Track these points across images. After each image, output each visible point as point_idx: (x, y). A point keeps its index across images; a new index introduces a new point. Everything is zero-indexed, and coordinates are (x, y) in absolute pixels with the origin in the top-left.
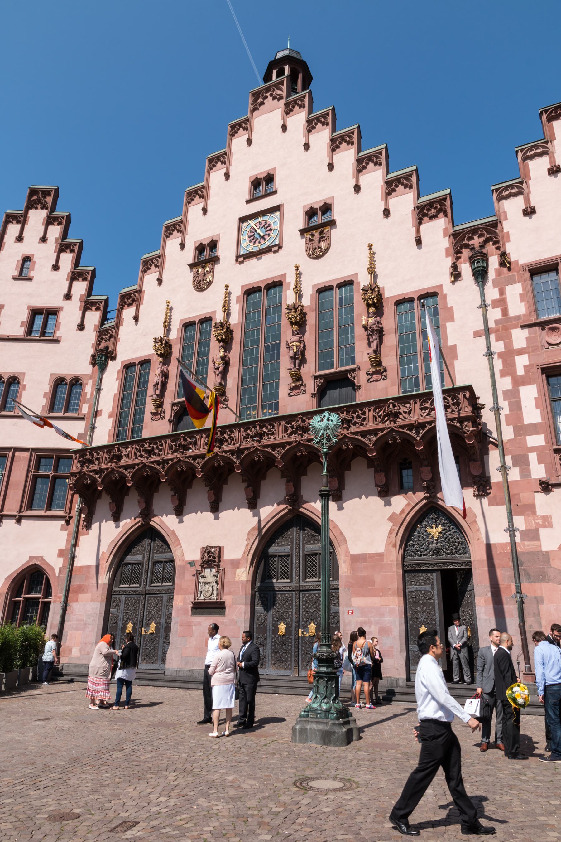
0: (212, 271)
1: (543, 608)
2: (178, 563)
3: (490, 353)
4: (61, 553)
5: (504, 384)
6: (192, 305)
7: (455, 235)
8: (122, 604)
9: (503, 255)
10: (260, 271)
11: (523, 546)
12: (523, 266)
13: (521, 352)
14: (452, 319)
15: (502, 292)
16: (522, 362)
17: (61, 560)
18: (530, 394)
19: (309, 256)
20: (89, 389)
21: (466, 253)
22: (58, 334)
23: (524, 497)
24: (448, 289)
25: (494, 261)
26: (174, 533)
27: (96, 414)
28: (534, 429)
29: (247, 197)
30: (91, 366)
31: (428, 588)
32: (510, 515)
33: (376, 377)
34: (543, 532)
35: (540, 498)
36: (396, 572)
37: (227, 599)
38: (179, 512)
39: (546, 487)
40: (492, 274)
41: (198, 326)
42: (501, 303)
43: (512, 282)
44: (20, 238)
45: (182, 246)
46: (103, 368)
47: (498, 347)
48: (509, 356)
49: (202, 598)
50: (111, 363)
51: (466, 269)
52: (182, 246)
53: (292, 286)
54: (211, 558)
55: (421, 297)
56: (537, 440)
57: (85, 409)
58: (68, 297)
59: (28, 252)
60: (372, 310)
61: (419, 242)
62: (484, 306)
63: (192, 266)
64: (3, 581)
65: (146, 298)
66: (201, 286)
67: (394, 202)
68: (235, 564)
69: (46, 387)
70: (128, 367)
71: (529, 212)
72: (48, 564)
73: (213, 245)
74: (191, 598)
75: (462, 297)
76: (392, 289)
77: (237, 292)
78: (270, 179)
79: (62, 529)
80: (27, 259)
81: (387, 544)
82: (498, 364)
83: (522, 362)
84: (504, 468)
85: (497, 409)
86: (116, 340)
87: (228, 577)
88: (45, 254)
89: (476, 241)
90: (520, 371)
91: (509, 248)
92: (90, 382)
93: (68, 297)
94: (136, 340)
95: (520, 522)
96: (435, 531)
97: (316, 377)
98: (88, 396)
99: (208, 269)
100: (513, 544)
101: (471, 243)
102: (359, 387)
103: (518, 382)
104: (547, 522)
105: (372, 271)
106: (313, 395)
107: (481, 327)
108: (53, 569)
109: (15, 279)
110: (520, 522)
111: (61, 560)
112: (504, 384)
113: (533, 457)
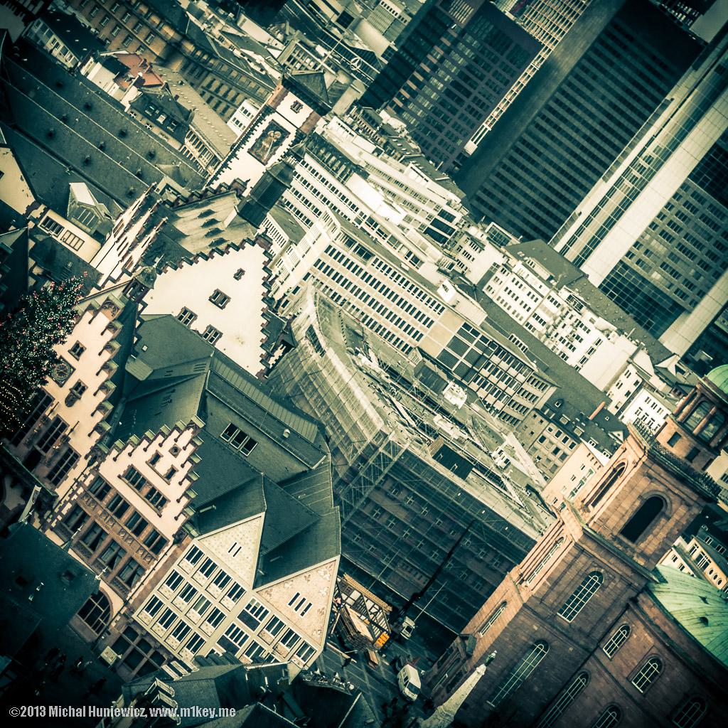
3: (71, 487)
5: (67, 498)
7: (96, 445)
9: (98, 466)
16: (75, 497)
18: (69, 506)
21: (94, 454)
25: (96, 463)
28: (61, 515)
40: (92, 467)
42: (86, 477)
47: (75, 488)
48: (74, 492)
56: (60, 518)
62: (82, 473)
67: (98, 412)
71: (115, 459)
75: (82, 464)
78: (82, 350)
82: (70, 492)
84: (48, 517)
85: (60, 502)
89: (99, 453)
91: (102, 464)
103: (70, 501)
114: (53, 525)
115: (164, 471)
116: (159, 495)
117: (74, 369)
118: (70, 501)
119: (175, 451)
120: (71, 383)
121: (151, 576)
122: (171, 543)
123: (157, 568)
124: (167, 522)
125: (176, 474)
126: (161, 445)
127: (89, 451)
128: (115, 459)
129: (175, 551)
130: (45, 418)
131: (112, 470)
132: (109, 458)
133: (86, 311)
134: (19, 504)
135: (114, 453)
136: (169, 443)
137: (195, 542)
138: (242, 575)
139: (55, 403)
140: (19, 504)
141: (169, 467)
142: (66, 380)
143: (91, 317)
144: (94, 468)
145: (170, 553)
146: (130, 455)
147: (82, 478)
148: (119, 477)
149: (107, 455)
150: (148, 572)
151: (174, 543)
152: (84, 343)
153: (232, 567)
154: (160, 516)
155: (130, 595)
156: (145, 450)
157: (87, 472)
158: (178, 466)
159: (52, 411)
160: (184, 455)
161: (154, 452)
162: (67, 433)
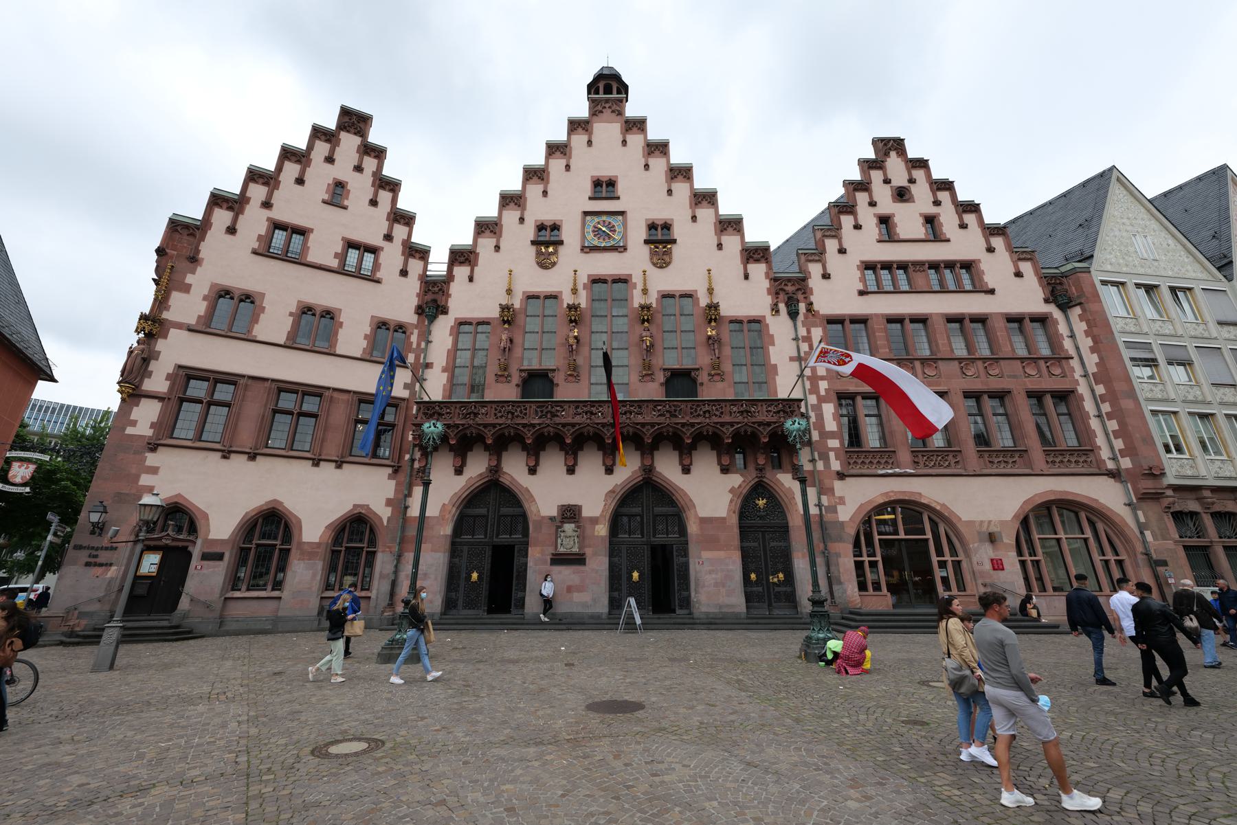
0: (555, 253)
1: (841, 560)
2: (532, 518)
3: (801, 376)
4: (389, 502)
6: (534, 280)
8: (465, 554)
10: (607, 265)
11: (828, 517)
12: (823, 316)
13: (822, 378)
14: (773, 344)
15: (809, 331)
16: (823, 385)
17: (389, 510)
18: (829, 409)
19: (654, 264)
20: (414, 338)
21: (782, 296)
22: (379, 275)
23: (827, 482)
24: (770, 320)
25: (802, 307)
26: (527, 490)
27: (428, 366)
29: (589, 193)
30: (416, 317)
31: (756, 544)
32: (820, 494)
33: (716, 378)
34: (839, 508)
35: (838, 485)
36: (736, 531)
37: (588, 551)
38: (532, 471)
39: (841, 476)
40: (801, 317)
41: (541, 301)
42: (808, 339)
43: (816, 326)
44: (330, 160)
45: (522, 220)
46: (432, 318)
49: (562, 550)
50: (441, 318)
51: (782, 306)
52: (522, 220)
53: (640, 286)
54: (570, 513)
55: (750, 322)
56: (834, 443)
57: (411, 358)
58: (388, 237)
59: (341, 178)
60: (713, 324)
61: (746, 277)
62: (796, 339)
63: (533, 243)
64: (323, 529)
65: (481, 260)
66: (545, 263)
68: (594, 521)
69: (368, 330)
70: (461, 323)
72: (375, 514)
73: (555, 227)
74: (551, 550)
76: (726, 310)
77: (583, 279)
78: (611, 183)
79: (390, 477)
80: (339, 186)
81: (729, 511)
83: (823, 385)
84: (813, 461)
86: (449, 296)
87: (588, 532)
88: (360, 186)
89: (790, 288)
90: (823, 393)
91: (813, 299)
92: (416, 332)
93: (388, 237)
94: (472, 299)
95: (825, 500)
96: (761, 502)
97: (665, 370)
98: (414, 346)
99: (551, 249)
100: (821, 515)
101: (787, 288)
102: (702, 384)
103: (821, 400)
104: (842, 501)
105: (710, 291)
106: (662, 384)
107: (795, 354)
108: (380, 519)
109: (324, 202)
110: (825, 500)
111: (389, 510)
112: (812, 399)
113: (832, 455)
114: (836, 465)
115: (920, 231)
116: (950, 265)
117: (622, 213)
118: (821, 400)
119: (902, 195)
120: (637, 234)
121: (1100, 389)
122: (1057, 314)
123: (1092, 369)
124: (1016, 291)
125: (942, 219)
126: (872, 204)
127: (769, 300)
128: (826, 276)
129: (1081, 318)
130: (645, 307)
131: (837, 292)
132: (815, 282)
133: (569, 134)
134: (732, 491)
135: (815, 269)
136: (882, 194)
137: (1097, 277)
138: (1193, 275)
139: (637, 279)
140: (732, 491)
141: (921, 220)
142: (625, 237)
143: (585, 138)
144: (806, 317)
145: (1080, 327)
146: (842, 251)
147: (804, 347)
148: (861, 293)
149: (804, 280)
150: (1083, 389)
151: (1064, 307)
152: (605, 172)
153: (1170, 273)
154: (992, 292)
155: (1105, 454)
156: (857, 227)
157: (802, 332)
158: (933, 210)
159: (645, 291)
160: (921, 191)
161: (875, 221)
162: (704, 301)
